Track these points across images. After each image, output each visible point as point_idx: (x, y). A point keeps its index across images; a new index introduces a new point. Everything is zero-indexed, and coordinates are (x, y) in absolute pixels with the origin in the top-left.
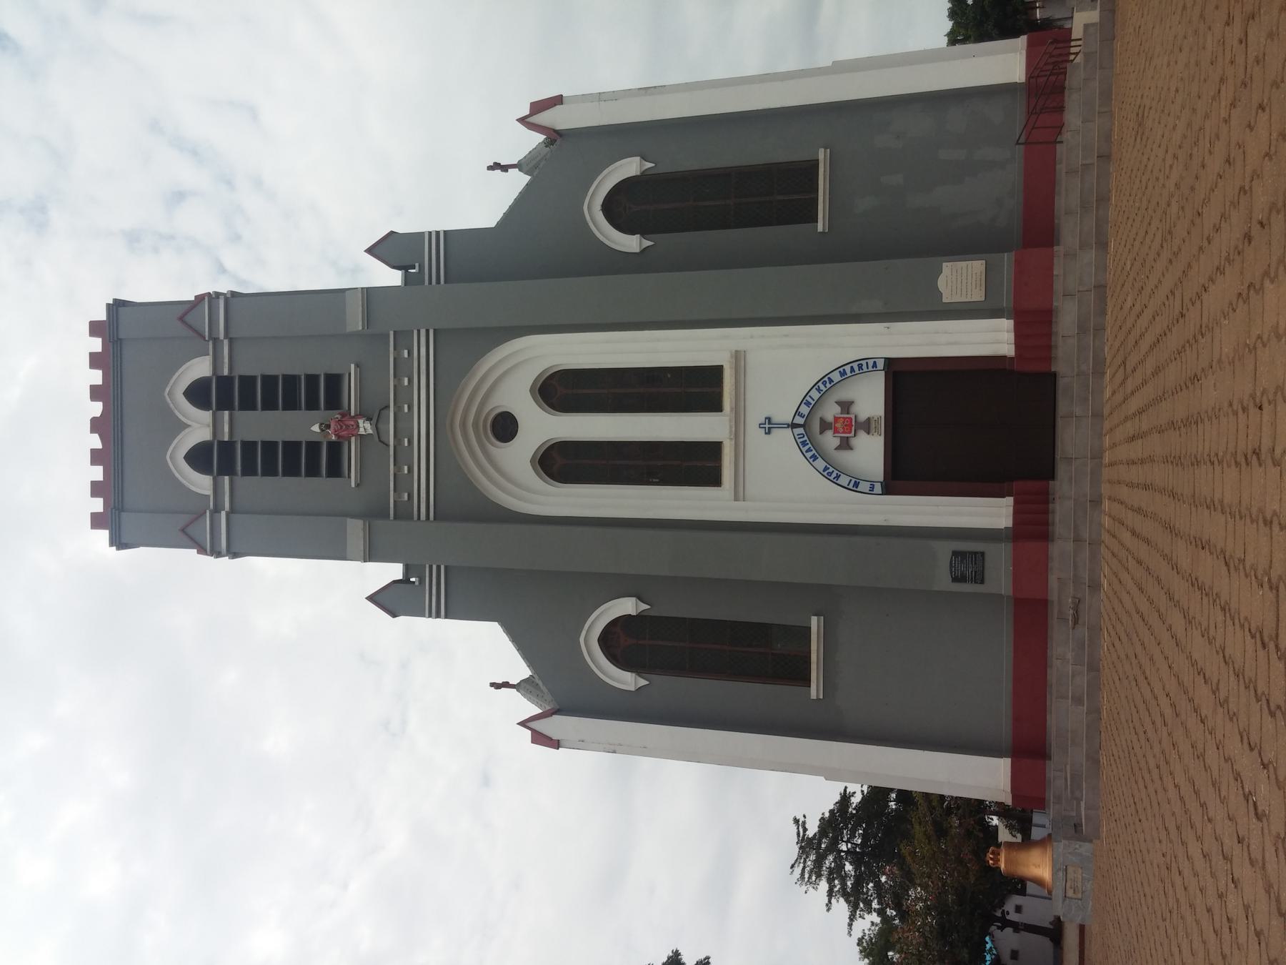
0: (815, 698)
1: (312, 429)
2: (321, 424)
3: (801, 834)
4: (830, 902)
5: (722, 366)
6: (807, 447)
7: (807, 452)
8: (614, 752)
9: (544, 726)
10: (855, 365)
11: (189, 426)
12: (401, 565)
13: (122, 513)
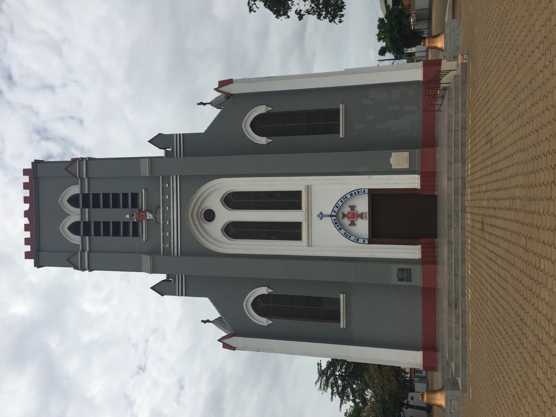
0: (342, 328)
1: (126, 216)
2: (130, 215)
3: (319, 369)
4: (332, 397)
5: (301, 191)
6: (337, 225)
7: (337, 226)
8: (259, 351)
9: (228, 341)
10: (356, 192)
11: (70, 215)
12: (166, 274)
13: (40, 253)
